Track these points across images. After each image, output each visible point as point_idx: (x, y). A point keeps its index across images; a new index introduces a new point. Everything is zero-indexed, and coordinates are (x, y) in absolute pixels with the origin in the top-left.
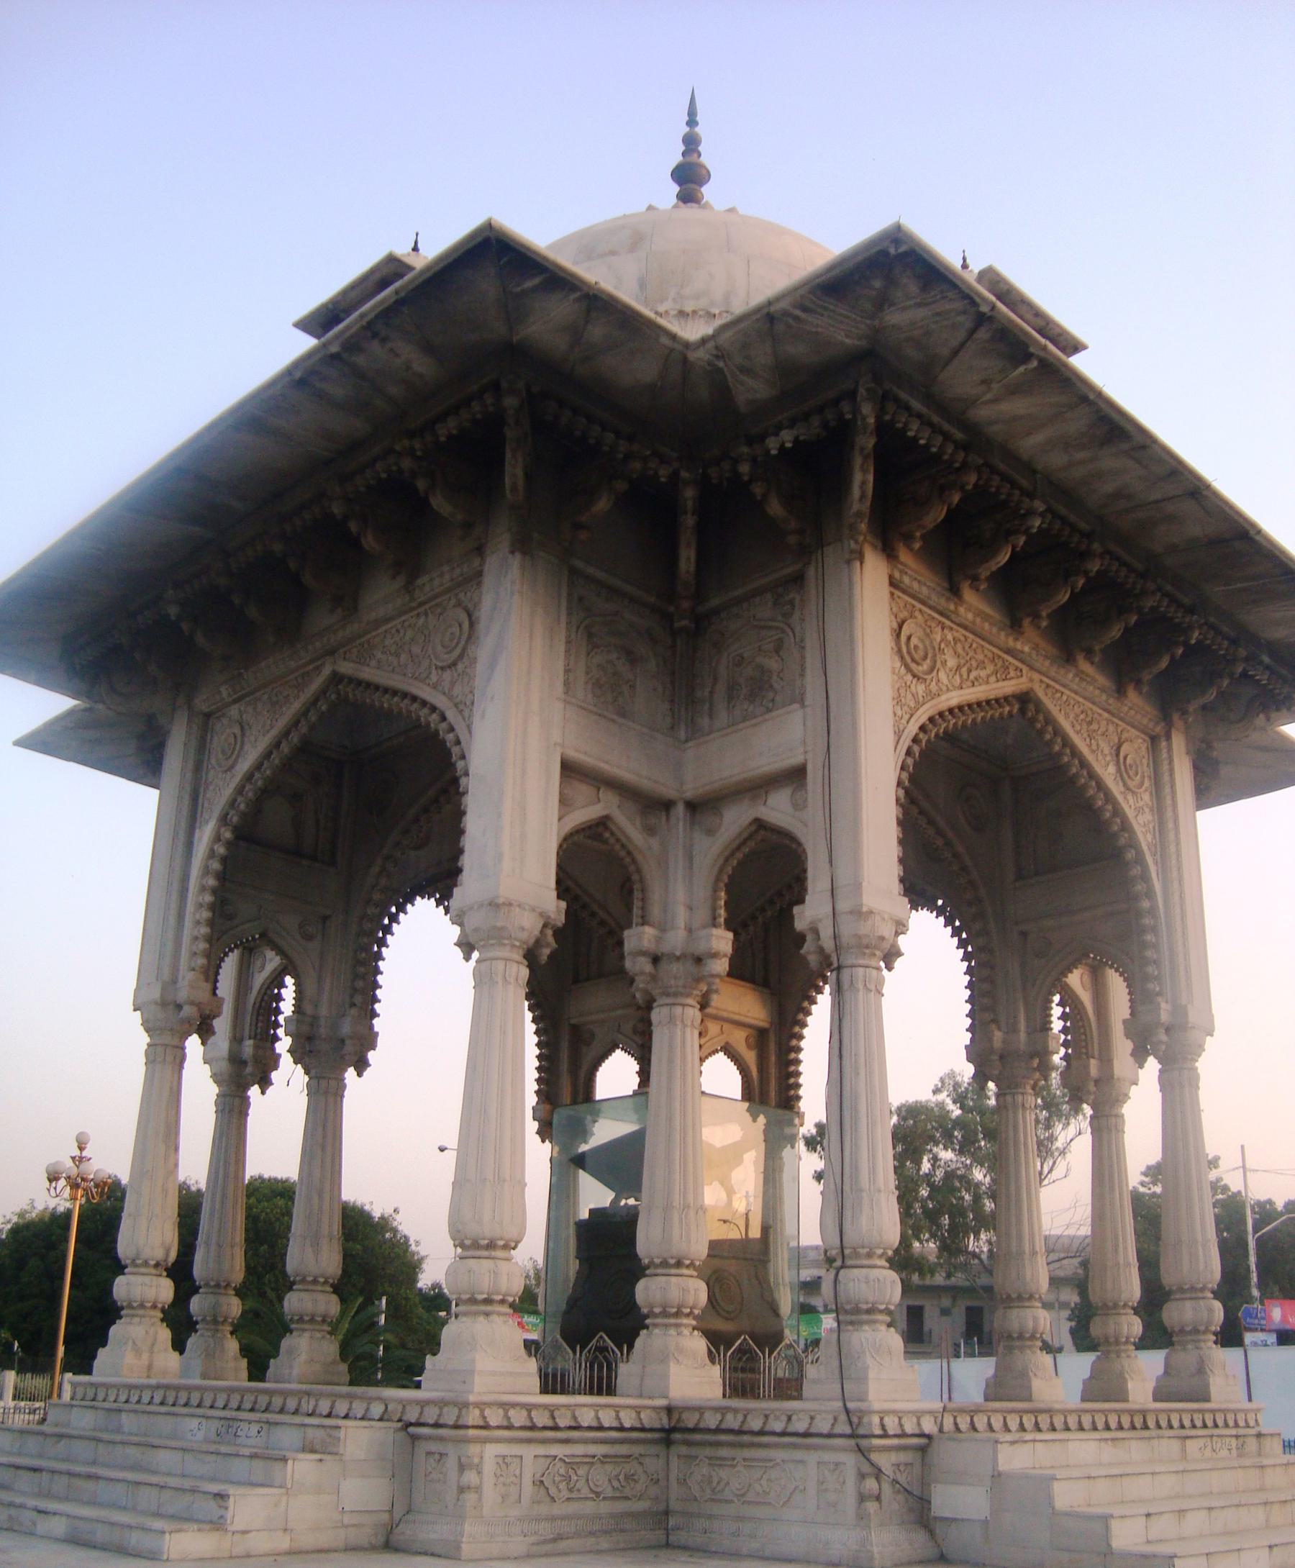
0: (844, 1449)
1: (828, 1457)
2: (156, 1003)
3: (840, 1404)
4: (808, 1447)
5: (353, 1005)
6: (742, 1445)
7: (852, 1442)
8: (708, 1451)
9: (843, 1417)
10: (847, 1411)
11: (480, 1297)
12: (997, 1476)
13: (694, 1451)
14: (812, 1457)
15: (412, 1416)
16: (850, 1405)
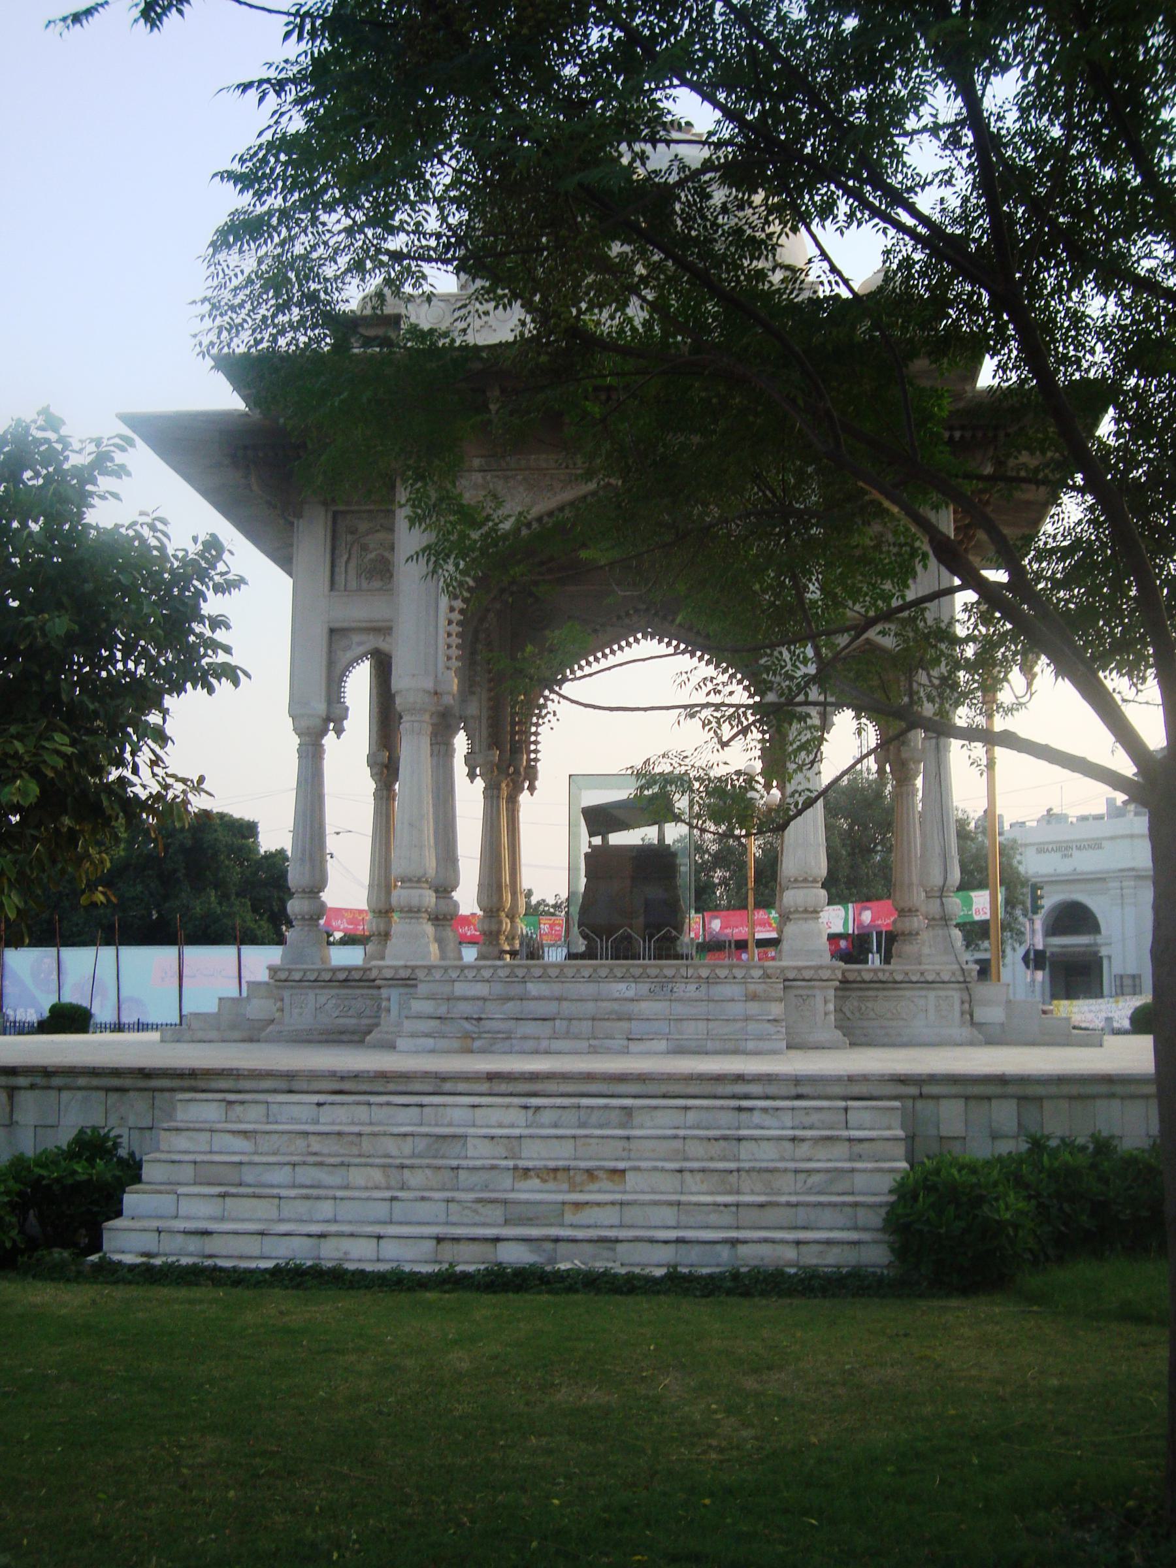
0: (953, 989)
1: (942, 993)
2: (429, 692)
3: (956, 967)
4: (929, 989)
5: (473, 693)
6: (884, 989)
7: (962, 986)
8: (859, 993)
9: (959, 973)
10: (963, 970)
11: (800, 909)
12: (1009, 1002)
13: (848, 993)
14: (932, 995)
15: (791, 975)
16: (965, 967)
